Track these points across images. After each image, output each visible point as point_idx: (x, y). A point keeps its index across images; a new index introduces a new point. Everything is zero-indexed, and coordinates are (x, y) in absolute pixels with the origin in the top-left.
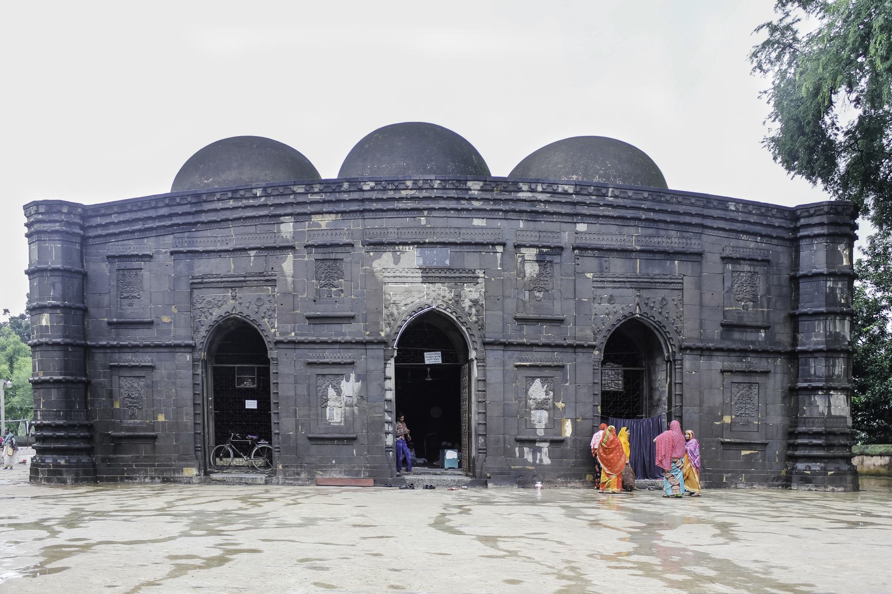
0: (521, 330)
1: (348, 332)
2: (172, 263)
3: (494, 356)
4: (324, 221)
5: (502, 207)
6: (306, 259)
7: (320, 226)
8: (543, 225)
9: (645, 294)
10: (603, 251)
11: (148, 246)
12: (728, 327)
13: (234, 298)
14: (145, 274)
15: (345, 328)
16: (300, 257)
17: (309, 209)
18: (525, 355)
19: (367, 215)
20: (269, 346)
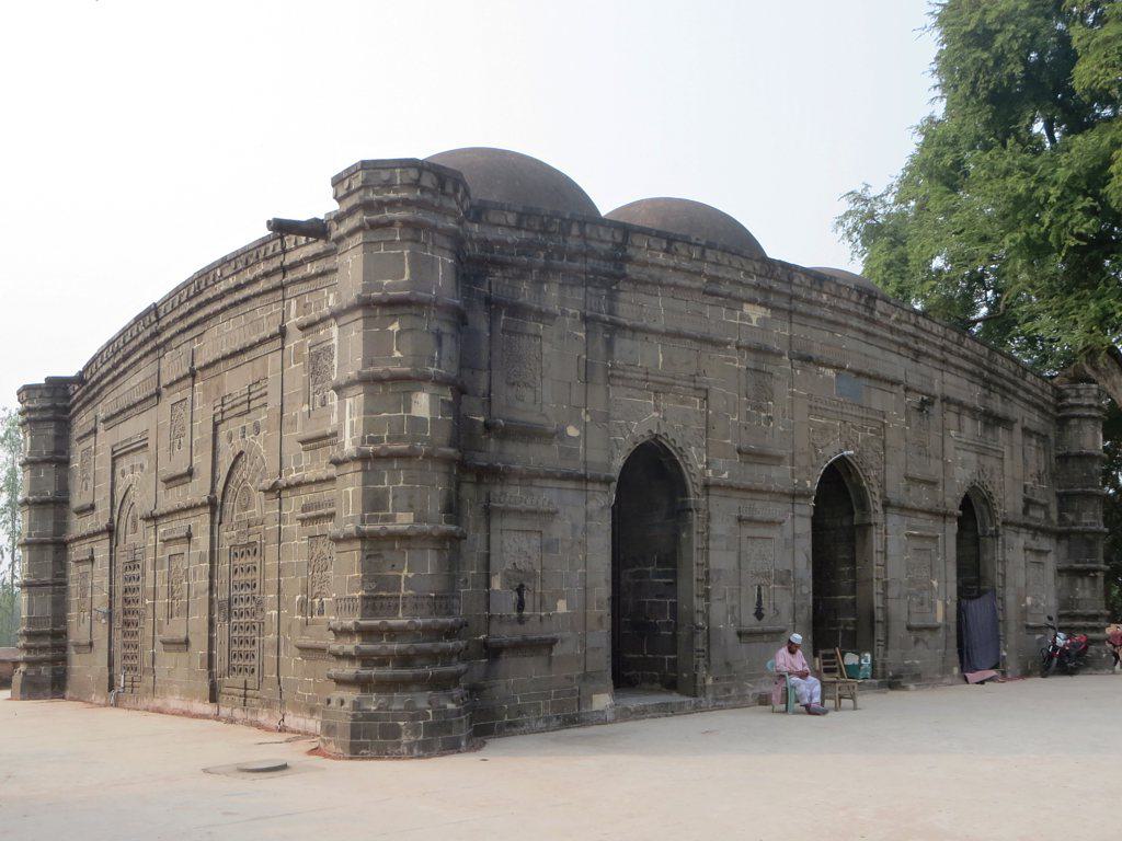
1: (779, 476)
2: (582, 335)
4: (755, 313)
5: (896, 338)
6: (737, 365)
7: (750, 320)
8: (925, 367)
9: (982, 458)
11: (552, 295)
13: (657, 408)
14: (547, 348)
15: (775, 472)
16: (731, 360)
17: (741, 292)
19: (795, 318)
20: (694, 489)
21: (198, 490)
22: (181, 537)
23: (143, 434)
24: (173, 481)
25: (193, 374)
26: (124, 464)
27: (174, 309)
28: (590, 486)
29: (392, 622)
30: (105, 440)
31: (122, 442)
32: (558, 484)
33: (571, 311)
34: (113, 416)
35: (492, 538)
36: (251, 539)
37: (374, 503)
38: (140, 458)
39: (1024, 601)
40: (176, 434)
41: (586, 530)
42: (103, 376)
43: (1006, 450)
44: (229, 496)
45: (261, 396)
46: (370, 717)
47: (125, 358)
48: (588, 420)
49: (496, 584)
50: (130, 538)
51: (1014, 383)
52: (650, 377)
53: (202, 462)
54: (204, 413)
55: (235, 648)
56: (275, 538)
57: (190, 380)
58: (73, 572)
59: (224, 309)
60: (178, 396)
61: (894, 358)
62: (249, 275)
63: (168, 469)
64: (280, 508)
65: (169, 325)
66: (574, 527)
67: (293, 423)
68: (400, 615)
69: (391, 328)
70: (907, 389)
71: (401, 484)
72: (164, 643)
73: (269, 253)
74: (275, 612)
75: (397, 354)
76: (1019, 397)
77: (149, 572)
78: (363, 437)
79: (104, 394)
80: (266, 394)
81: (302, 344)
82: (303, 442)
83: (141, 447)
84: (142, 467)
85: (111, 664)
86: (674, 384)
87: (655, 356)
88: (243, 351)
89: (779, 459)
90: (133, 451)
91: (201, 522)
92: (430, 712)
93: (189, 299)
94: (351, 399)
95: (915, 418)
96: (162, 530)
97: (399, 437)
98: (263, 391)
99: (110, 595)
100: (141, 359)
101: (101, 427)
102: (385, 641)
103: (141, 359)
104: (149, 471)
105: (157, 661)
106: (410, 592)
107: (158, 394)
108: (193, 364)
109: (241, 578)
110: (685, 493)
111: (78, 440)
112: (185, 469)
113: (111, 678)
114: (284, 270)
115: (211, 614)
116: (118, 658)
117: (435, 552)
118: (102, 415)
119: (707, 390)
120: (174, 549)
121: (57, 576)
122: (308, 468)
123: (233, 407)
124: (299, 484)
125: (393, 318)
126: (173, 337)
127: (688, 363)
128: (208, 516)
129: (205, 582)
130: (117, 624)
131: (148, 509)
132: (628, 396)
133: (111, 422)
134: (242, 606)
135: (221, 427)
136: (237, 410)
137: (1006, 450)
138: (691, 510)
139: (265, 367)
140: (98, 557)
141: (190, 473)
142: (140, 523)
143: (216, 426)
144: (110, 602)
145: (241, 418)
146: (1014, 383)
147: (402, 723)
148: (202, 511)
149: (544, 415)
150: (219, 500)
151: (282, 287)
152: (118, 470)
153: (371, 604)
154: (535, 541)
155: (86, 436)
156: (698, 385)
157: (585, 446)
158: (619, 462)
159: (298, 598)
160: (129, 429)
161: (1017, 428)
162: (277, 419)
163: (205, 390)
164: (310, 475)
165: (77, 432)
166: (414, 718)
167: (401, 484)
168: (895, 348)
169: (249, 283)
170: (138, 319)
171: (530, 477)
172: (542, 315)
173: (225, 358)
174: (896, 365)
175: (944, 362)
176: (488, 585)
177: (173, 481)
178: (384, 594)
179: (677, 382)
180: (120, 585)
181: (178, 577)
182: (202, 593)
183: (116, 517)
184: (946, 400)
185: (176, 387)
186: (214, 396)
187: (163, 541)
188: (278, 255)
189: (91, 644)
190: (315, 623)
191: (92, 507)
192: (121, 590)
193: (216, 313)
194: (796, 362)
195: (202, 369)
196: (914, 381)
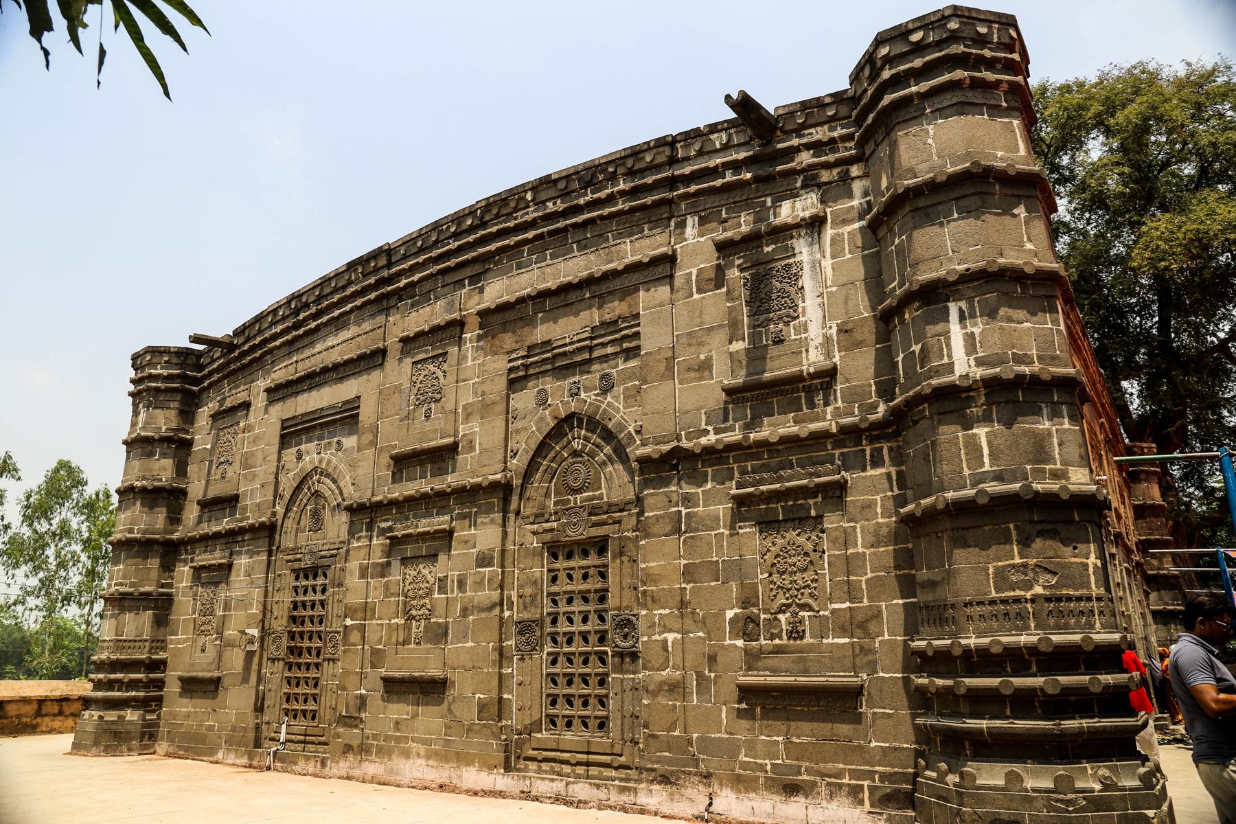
23: (348, 402)
31: (304, 415)
47: (315, 316)
75: (1029, 246)
80: (637, 334)
93: (456, 236)
114: (672, 183)
121: (163, 586)
125: (1015, 200)
133: (281, 394)
159: (730, 614)
170: (351, 266)
191: (234, 499)
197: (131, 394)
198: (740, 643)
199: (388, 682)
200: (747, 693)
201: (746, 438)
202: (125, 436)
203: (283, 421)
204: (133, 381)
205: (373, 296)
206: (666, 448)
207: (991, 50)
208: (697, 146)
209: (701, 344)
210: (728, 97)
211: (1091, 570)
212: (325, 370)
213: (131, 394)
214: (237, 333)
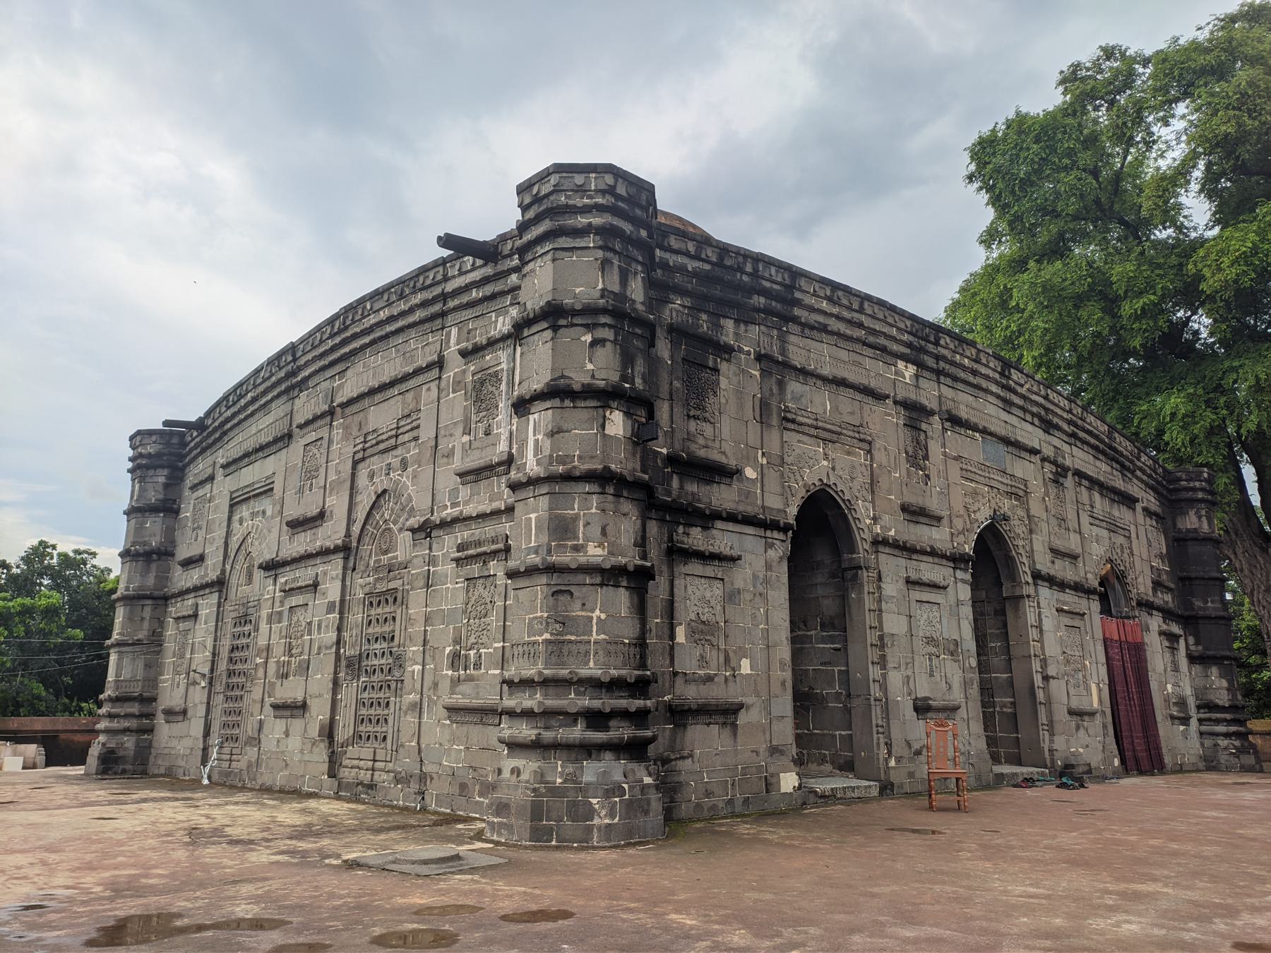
0: (1053, 562)
1: (938, 537)
2: (757, 373)
3: (1045, 592)
10: (1095, 484)
12: (1157, 585)
13: (826, 458)
14: (724, 382)
17: (895, 347)
18: (1062, 596)
20: (863, 546)
21: (331, 533)
22: (306, 586)
23: (268, 478)
24: (297, 525)
25: (331, 413)
26: (244, 511)
27: (314, 347)
28: (769, 534)
29: (584, 672)
30: (224, 487)
31: (243, 488)
32: (738, 528)
33: (746, 349)
34: (235, 461)
35: (676, 582)
36: (392, 585)
37: (561, 529)
38: (266, 505)
39: (1166, 689)
40: (310, 474)
41: (766, 581)
42: (227, 420)
43: (1132, 528)
44: (367, 539)
45: (412, 429)
46: (554, 791)
48: (765, 462)
49: (681, 635)
50: (239, 589)
51: (1132, 462)
52: (820, 424)
53: (337, 504)
54: (342, 449)
55: (364, 711)
56: (422, 582)
57: (328, 419)
58: (170, 631)
59: (373, 342)
60: (313, 436)
61: (1029, 428)
62: (403, 306)
63: (293, 512)
64: (430, 549)
65: (307, 364)
66: (755, 577)
67: (450, 455)
68: (591, 664)
69: (583, 339)
70: (1043, 460)
71: (594, 511)
72: (275, 707)
73: (428, 282)
74: (418, 668)
75: (590, 366)
76: (1137, 478)
77: (264, 627)
78: (551, 456)
79: (226, 439)
80: (418, 427)
81: (464, 372)
82: (461, 475)
83: (265, 492)
84: (264, 512)
85: (207, 734)
86: (840, 434)
87: (821, 403)
88: (392, 384)
89: (939, 519)
90: (255, 496)
91: (334, 567)
92: (626, 786)
93: (332, 336)
94: (536, 416)
95: (1053, 490)
96: (283, 580)
97: (592, 457)
98: (414, 424)
99: (214, 654)
100: (272, 400)
101: (220, 473)
102: (573, 696)
103: (272, 400)
104: (272, 517)
105: (265, 730)
106: (603, 636)
107: (289, 436)
108: (332, 401)
109: (376, 630)
110: (852, 549)
111: (191, 488)
112: (315, 511)
113: (205, 750)
114: (444, 297)
115: (336, 673)
116: (216, 727)
117: (627, 593)
118: (222, 461)
119: (870, 443)
120: (295, 600)
122: (466, 503)
123: (377, 444)
124: (455, 520)
126: (311, 376)
127: (852, 413)
128: (341, 562)
129: (332, 636)
130: (219, 688)
131: (268, 556)
132: (799, 441)
133: (233, 468)
134: (376, 662)
135: (360, 466)
136: (382, 446)
137: (1132, 528)
138: (860, 568)
139: (417, 399)
140: (203, 613)
141: (321, 516)
142: (258, 575)
143: (355, 464)
144: (213, 662)
145: (385, 455)
146: (1132, 462)
147: (594, 801)
148: (333, 557)
149: (724, 453)
150: (354, 544)
151: (443, 314)
152: (236, 518)
153: (557, 648)
154: (717, 590)
155: (202, 483)
156: (862, 436)
157: (762, 490)
158: (793, 511)
159: (448, 650)
160: (250, 475)
161: (1139, 506)
162: (428, 453)
163: (346, 428)
164: (471, 510)
165: (190, 480)
166: (608, 794)
167: (594, 511)
168: (1029, 417)
169: (403, 314)
171: (708, 518)
172: (727, 351)
173: (372, 392)
174: (1031, 435)
175: (1073, 435)
176: (672, 636)
177: (297, 525)
178: (573, 638)
179: (845, 432)
180: (226, 643)
181: (302, 632)
182: (327, 648)
183: (228, 567)
184: (1078, 474)
185: (311, 427)
186: (355, 432)
187: (284, 591)
188: (439, 283)
189: (184, 712)
190: (470, 679)
191: (201, 559)
192: (227, 648)
193: (363, 348)
194: (948, 425)
195: (344, 405)
196: (1048, 451)
197: (129, 471)
198: (450, 673)
199: (275, 707)
200: (452, 710)
201: (461, 512)
202: (126, 507)
203: (232, 493)
204: (130, 460)
205: (283, 387)
206: (422, 519)
207: (590, 197)
208: (457, 267)
209: (451, 435)
210: (439, 238)
211: (595, 621)
212: (257, 450)
213: (129, 471)
214: (208, 414)
